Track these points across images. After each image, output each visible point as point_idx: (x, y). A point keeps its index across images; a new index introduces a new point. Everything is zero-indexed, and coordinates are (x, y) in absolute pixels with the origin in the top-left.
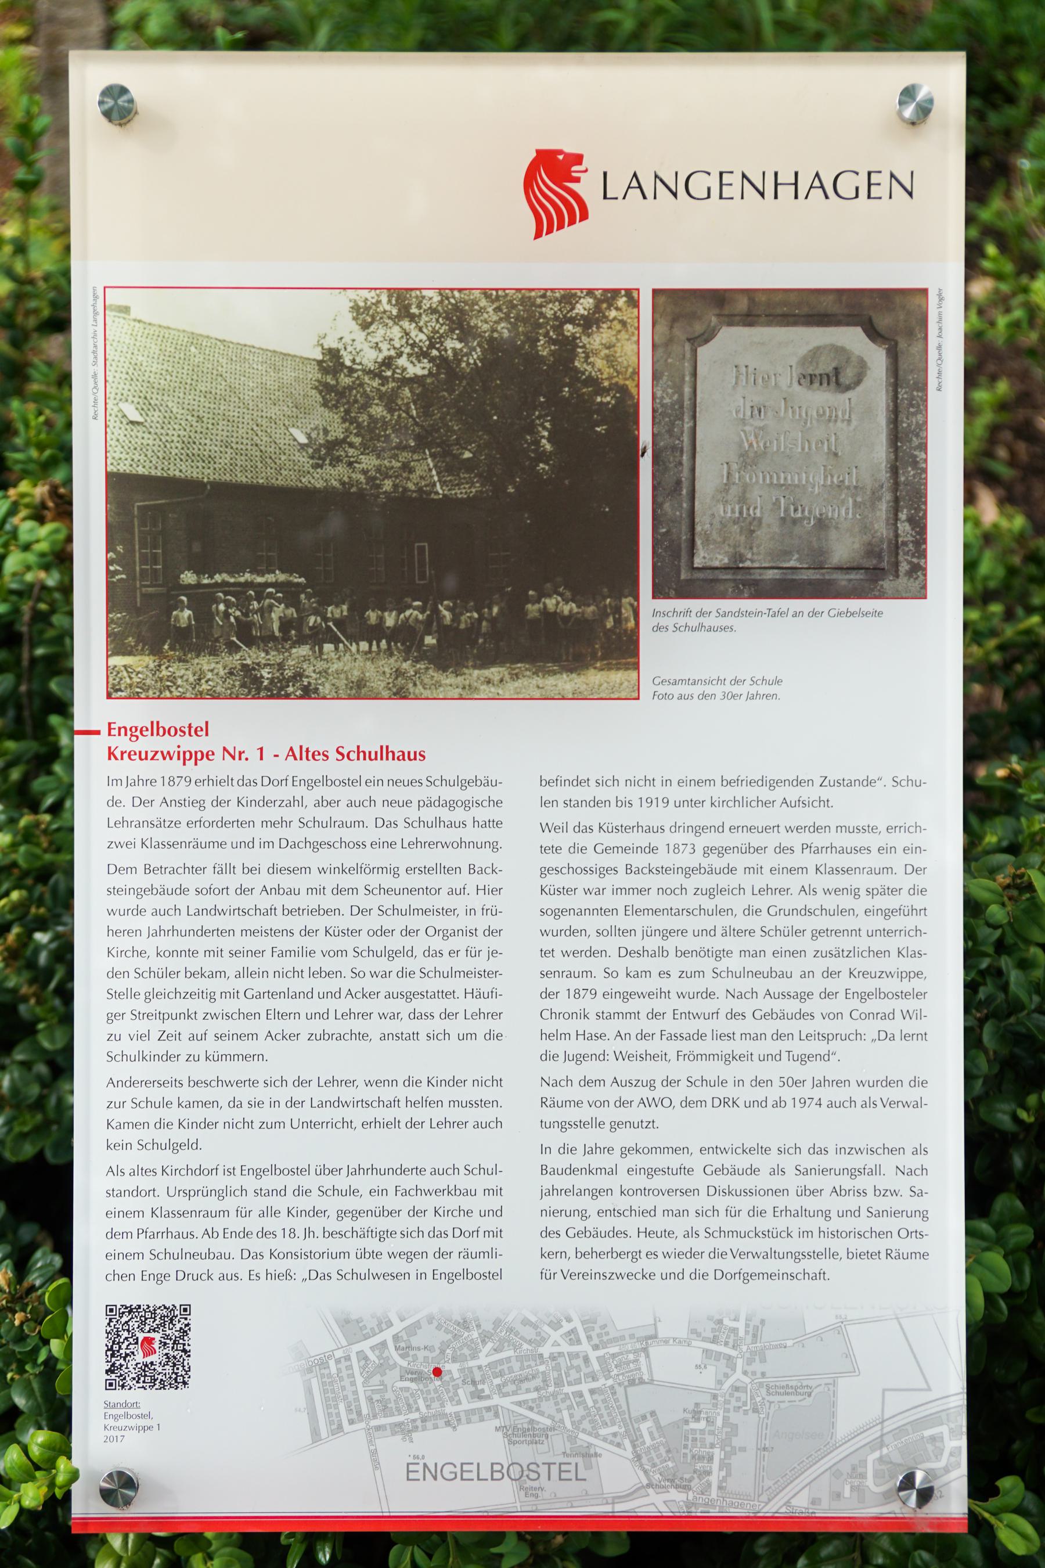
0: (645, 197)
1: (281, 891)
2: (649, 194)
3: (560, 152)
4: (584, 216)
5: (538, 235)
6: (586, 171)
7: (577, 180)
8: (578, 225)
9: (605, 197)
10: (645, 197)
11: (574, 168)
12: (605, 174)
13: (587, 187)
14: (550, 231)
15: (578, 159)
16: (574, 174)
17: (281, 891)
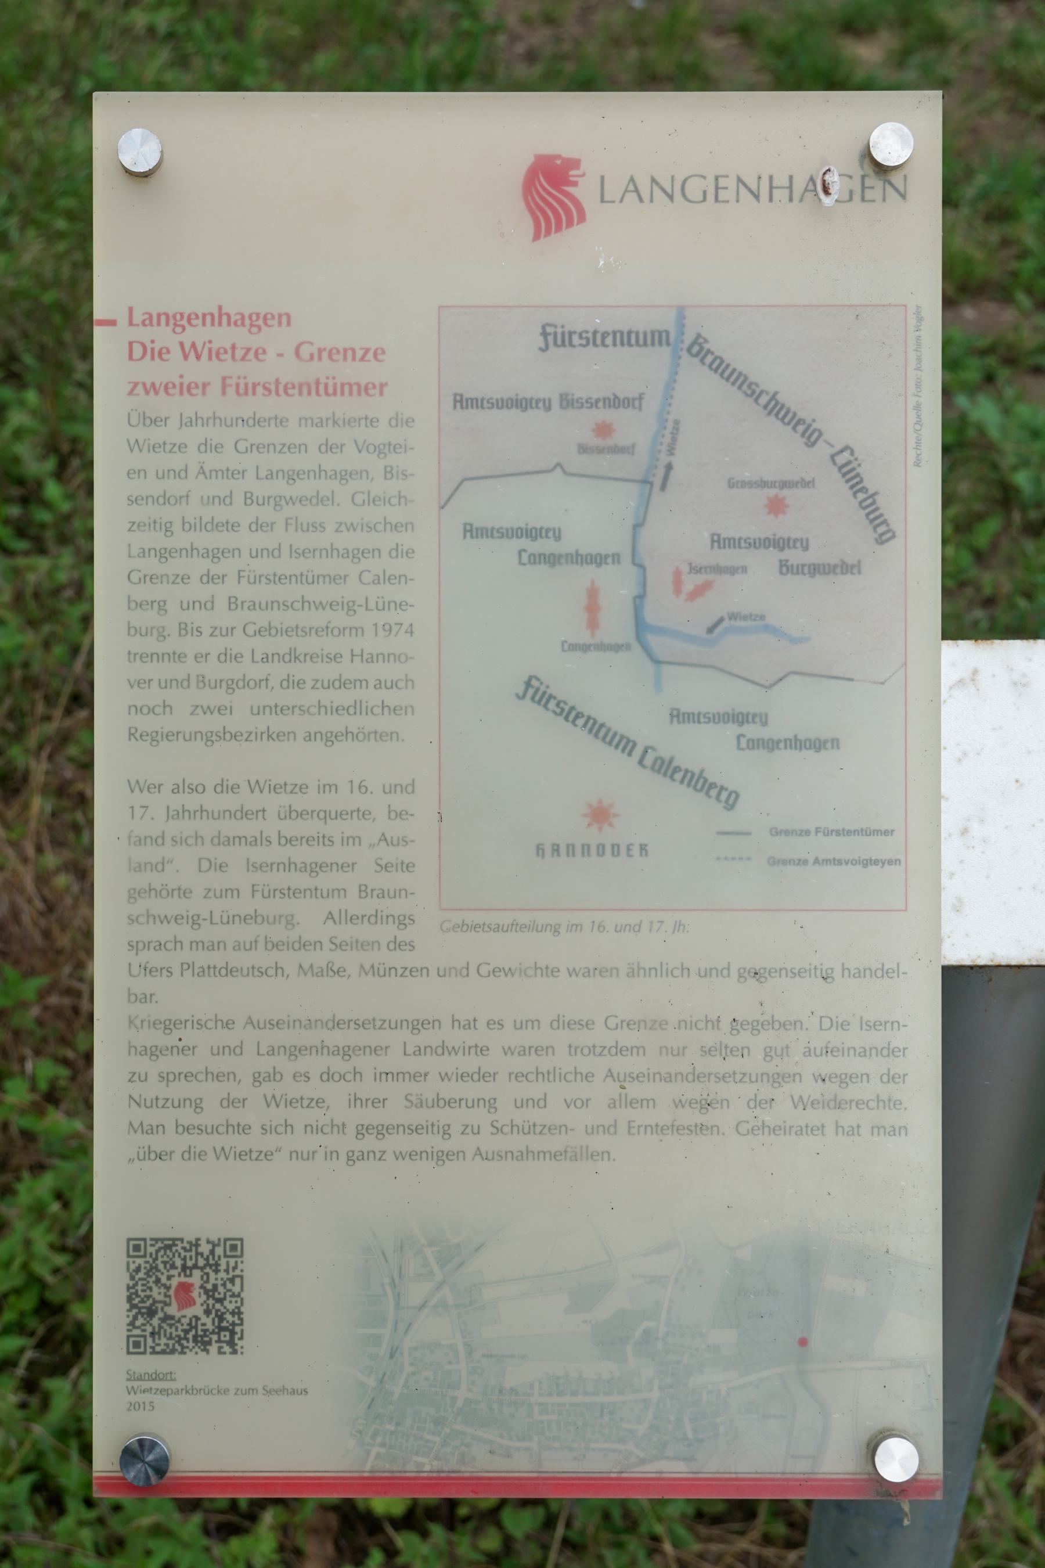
0: (641, 200)
1: (322, 815)
2: (646, 196)
3: (559, 157)
4: (582, 218)
5: (537, 237)
6: (583, 175)
7: (575, 184)
8: (576, 228)
9: (602, 201)
10: (641, 200)
11: (572, 173)
12: (602, 178)
13: (585, 191)
14: (548, 233)
15: (575, 163)
16: (572, 179)
17: (322, 815)
